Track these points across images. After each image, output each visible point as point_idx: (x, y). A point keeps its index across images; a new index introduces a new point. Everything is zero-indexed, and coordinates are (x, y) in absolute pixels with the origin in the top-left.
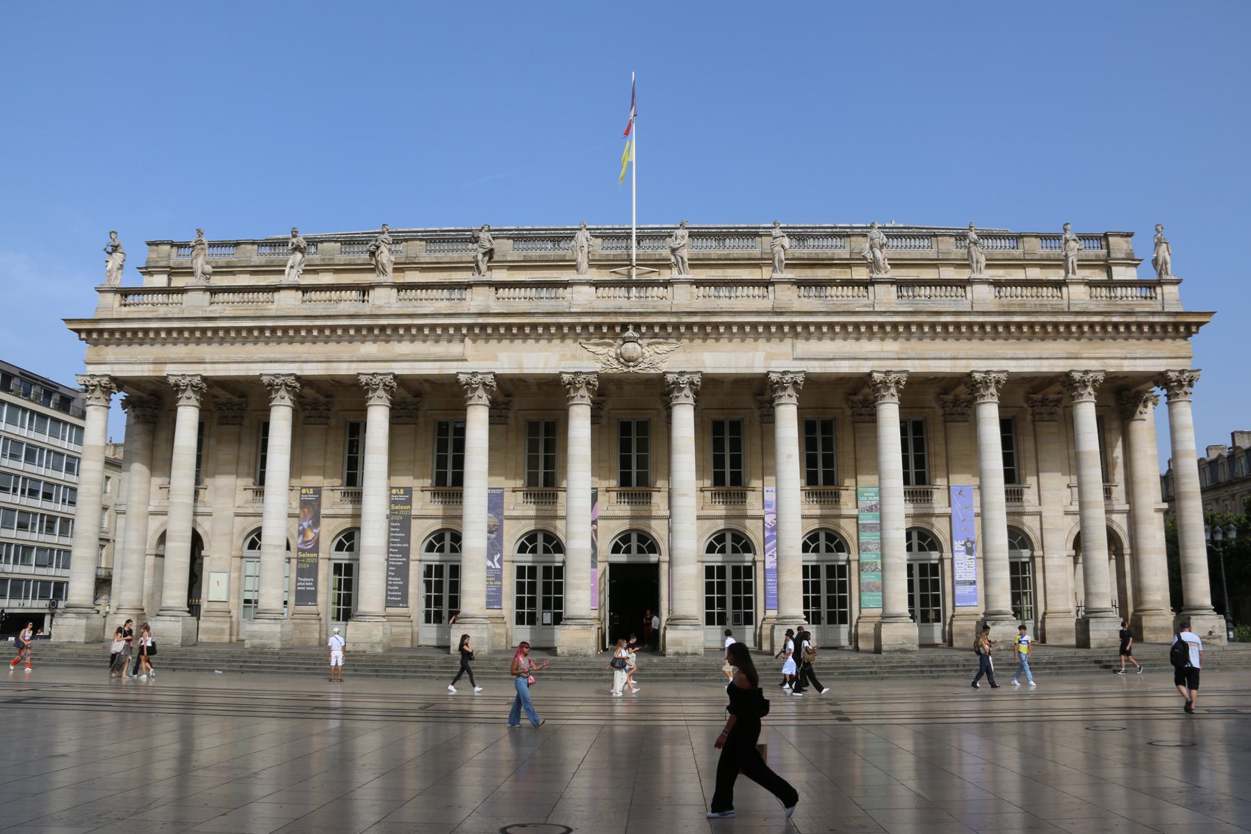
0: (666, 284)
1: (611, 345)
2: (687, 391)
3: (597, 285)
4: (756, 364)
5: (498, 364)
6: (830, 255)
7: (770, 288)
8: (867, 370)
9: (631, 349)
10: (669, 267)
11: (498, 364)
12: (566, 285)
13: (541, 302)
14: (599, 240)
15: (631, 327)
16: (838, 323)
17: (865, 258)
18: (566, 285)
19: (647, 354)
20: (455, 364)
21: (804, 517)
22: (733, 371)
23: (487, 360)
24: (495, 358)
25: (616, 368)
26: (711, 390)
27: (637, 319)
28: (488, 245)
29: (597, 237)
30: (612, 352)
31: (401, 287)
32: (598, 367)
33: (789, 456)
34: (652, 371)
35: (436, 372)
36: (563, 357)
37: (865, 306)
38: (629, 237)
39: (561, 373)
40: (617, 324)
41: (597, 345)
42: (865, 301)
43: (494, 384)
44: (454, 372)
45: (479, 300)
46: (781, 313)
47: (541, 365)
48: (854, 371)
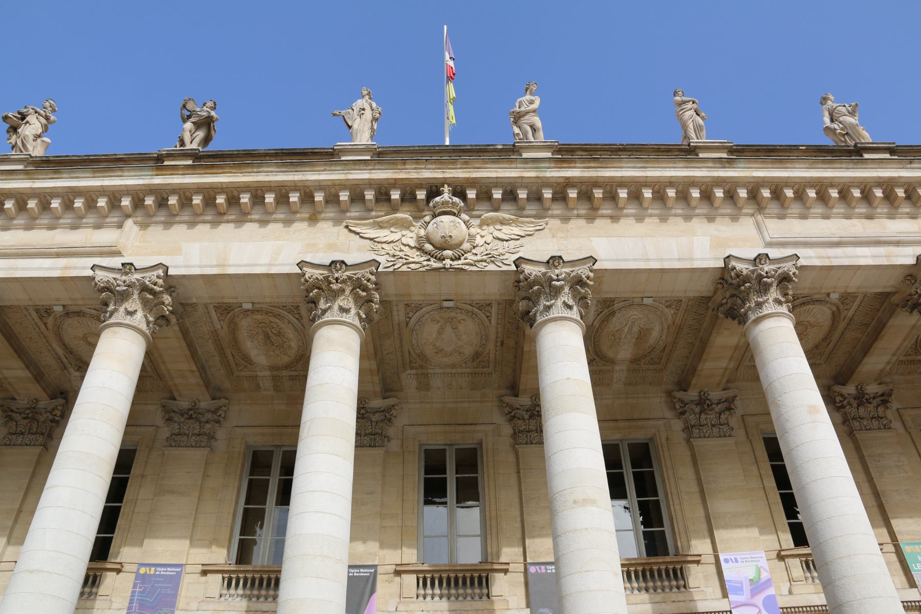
1: (406, 225)
2: (566, 296)
9: (448, 226)
15: (446, 189)
19: (479, 241)
30: (410, 238)
33: (813, 409)
34: (492, 267)
40: (420, 184)
41: (380, 226)
47: (265, 260)
48: (885, 262)
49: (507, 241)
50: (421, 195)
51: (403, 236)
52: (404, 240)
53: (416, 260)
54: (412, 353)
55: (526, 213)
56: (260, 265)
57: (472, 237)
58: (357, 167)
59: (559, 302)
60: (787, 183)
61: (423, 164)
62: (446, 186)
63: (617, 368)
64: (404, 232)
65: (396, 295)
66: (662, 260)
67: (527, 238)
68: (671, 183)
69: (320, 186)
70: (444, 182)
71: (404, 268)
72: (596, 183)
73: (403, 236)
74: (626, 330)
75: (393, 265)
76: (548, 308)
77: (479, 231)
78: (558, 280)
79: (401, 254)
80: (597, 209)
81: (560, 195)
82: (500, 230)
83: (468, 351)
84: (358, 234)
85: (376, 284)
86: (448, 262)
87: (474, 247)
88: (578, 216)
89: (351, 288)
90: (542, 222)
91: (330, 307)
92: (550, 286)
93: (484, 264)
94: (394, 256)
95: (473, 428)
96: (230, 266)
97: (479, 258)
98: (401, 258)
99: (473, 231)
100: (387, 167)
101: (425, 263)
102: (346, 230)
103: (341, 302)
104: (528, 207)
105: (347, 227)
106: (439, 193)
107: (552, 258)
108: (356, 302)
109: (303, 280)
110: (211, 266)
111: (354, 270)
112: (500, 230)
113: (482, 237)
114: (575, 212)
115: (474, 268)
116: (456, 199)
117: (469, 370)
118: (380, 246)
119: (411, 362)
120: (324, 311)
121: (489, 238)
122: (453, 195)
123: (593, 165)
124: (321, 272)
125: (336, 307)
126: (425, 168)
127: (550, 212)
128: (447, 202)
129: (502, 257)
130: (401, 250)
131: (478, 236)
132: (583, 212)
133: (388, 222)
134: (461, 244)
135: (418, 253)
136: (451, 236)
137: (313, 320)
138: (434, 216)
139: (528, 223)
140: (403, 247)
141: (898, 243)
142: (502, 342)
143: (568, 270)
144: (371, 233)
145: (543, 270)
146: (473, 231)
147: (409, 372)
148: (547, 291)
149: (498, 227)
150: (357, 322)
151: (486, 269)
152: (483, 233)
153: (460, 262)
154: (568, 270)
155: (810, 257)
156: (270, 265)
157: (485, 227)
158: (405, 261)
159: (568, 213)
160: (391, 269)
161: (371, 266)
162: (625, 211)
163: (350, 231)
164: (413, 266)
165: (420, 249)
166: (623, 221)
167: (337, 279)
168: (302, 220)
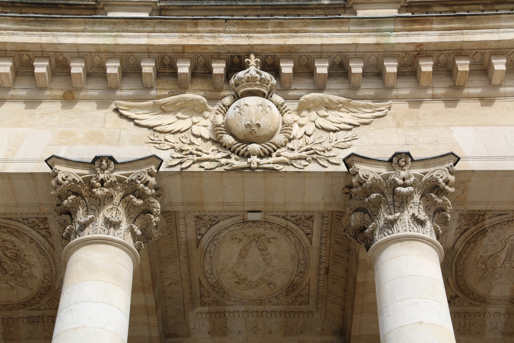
1: (198, 110)
2: (416, 208)
9: (253, 111)
15: (253, 60)
19: (297, 131)
30: (203, 126)
34: (313, 167)
39: (51, 161)
40: (217, 53)
41: (163, 110)
49: (335, 131)
50: (219, 68)
51: (194, 124)
52: (196, 130)
53: (212, 156)
54: (204, 282)
55: (361, 93)
57: (287, 127)
58: (131, 28)
59: (406, 216)
61: (222, 26)
62: (252, 56)
63: (491, 310)
64: (195, 119)
65: (183, 204)
67: (362, 127)
69: (79, 53)
70: (249, 50)
71: (195, 168)
72: (460, 51)
73: (194, 124)
74: (503, 256)
75: (181, 163)
76: (391, 224)
77: (297, 117)
78: (405, 186)
79: (191, 148)
80: (461, 87)
81: (409, 69)
82: (325, 117)
83: (281, 281)
84: (132, 120)
85: (156, 189)
86: (254, 160)
87: (290, 140)
88: (434, 98)
89: (121, 194)
90: (383, 106)
91: (91, 221)
92: (394, 193)
93: (303, 162)
94: (182, 151)
97: (296, 154)
98: (191, 153)
99: (288, 117)
100: (171, 28)
101: (224, 161)
102: (115, 115)
103: (108, 212)
104: (363, 86)
105: (116, 110)
106: (243, 66)
107: (396, 154)
108: (128, 213)
109: (53, 182)
111: (126, 169)
112: (325, 117)
113: (301, 126)
114: (430, 92)
116: (266, 75)
117: (281, 308)
118: (162, 137)
119: (202, 296)
120: (84, 226)
121: (310, 128)
122: (262, 69)
123: (456, 25)
124: (80, 171)
125: (100, 220)
126: (225, 32)
127: (394, 92)
128: (254, 79)
129: (327, 154)
131: (296, 126)
132: (440, 92)
133: (174, 104)
134: (272, 135)
135: (214, 147)
136: (258, 125)
137: (68, 238)
138: (237, 97)
139: (364, 107)
142: (327, 270)
143: (418, 171)
144: (151, 119)
145: (384, 171)
146: (288, 117)
147: (199, 309)
148: (390, 199)
149: (323, 112)
150: (129, 241)
151: (306, 169)
152: (302, 121)
153: (270, 160)
154: (418, 171)
157: (304, 113)
158: (196, 158)
159: (419, 94)
160: (177, 169)
161: (150, 164)
162: (502, 90)
163: (121, 116)
164: (207, 165)
165: (217, 142)
166: (498, 104)
167: (102, 182)
168: (53, 99)
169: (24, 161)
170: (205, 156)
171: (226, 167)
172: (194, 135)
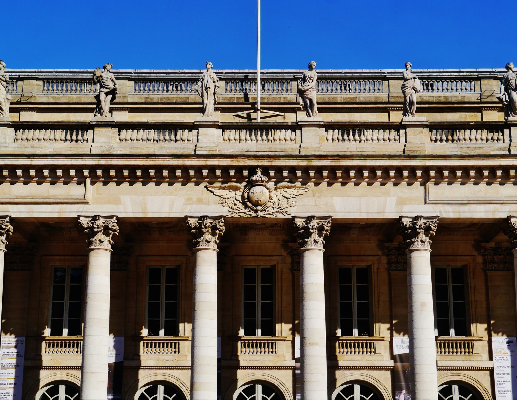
0: (295, 127)
3: (225, 127)
4: (388, 210)
5: (121, 208)
6: (460, 99)
7: (402, 132)
8: (504, 216)
10: (294, 111)
11: (121, 208)
12: (191, 127)
13: (167, 145)
14: (224, 82)
15: (259, 171)
16: (473, 167)
17: (500, 101)
18: (191, 127)
19: (275, 199)
20: (76, 206)
21: (439, 369)
22: (364, 216)
23: (109, 203)
24: (117, 202)
25: (244, 213)
26: (341, 234)
27: (266, 162)
28: (110, 85)
29: (221, 79)
31: (18, 126)
32: (224, 211)
34: (280, 216)
35: (56, 215)
36: (189, 200)
37: (502, 149)
38: (255, 79)
39: (187, 217)
42: (501, 144)
43: (117, 228)
44: (75, 215)
45: (104, 142)
46: (414, 157)
47: (166, 209)
50: (246, 173)
56: (165, 212)
60: (446, 168)
66: (368, 212)
68: (380, 167)
70: (257, 167)
78: (312, 229)
79: (236, 207)
84: (213, 192)
86: (259, 213)
93: (277, 214)
95: (271, 258)
96: (149, 212)
97: (275, 210)
101: (248, 213)
105: (206, 187)
110: (139, 212)
115: (272, 216)
118: (224, 200)
121: (280, 197)
129: (286, 210)
130: (235, 205)
140: (236, 201)
141: (502, 204)
153: (265, 213)
155: (449, 212)
156: (169, 212)
158: (238, 211)
163: (208, 190)
164: (241, 214)
169: (176, 212)
170: (241, 211)
171: (249, 216)
172: (236, 199)
